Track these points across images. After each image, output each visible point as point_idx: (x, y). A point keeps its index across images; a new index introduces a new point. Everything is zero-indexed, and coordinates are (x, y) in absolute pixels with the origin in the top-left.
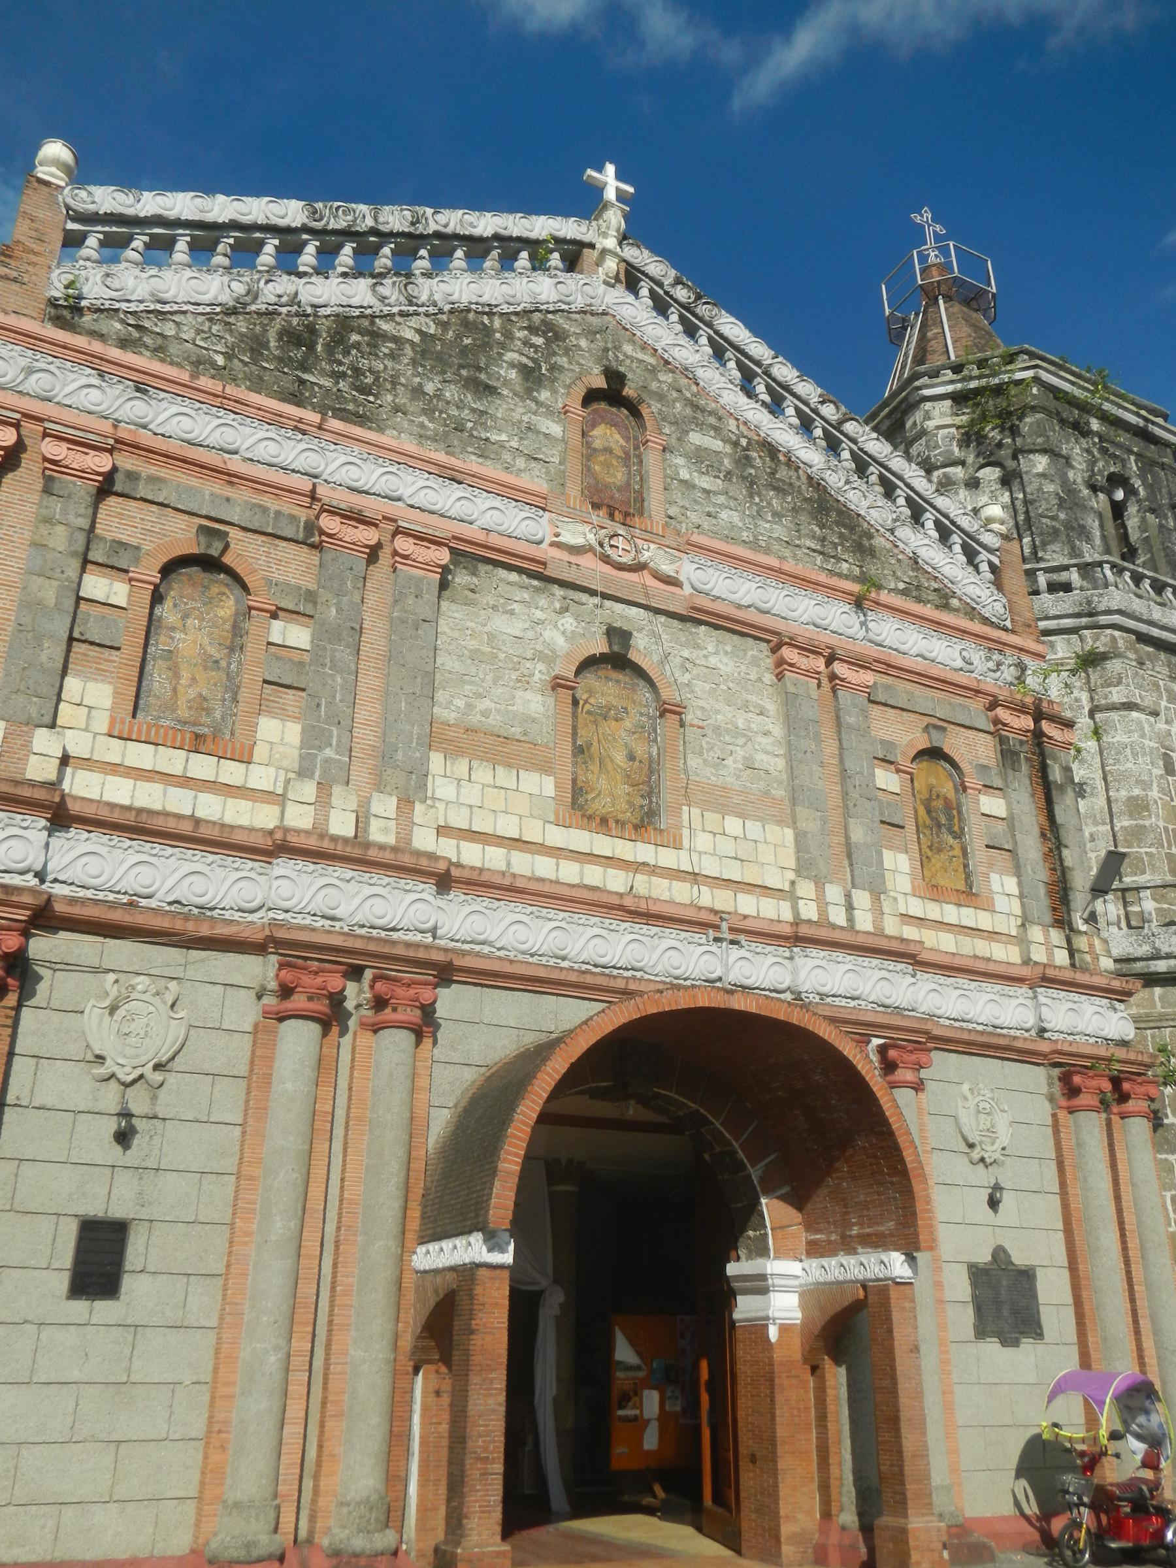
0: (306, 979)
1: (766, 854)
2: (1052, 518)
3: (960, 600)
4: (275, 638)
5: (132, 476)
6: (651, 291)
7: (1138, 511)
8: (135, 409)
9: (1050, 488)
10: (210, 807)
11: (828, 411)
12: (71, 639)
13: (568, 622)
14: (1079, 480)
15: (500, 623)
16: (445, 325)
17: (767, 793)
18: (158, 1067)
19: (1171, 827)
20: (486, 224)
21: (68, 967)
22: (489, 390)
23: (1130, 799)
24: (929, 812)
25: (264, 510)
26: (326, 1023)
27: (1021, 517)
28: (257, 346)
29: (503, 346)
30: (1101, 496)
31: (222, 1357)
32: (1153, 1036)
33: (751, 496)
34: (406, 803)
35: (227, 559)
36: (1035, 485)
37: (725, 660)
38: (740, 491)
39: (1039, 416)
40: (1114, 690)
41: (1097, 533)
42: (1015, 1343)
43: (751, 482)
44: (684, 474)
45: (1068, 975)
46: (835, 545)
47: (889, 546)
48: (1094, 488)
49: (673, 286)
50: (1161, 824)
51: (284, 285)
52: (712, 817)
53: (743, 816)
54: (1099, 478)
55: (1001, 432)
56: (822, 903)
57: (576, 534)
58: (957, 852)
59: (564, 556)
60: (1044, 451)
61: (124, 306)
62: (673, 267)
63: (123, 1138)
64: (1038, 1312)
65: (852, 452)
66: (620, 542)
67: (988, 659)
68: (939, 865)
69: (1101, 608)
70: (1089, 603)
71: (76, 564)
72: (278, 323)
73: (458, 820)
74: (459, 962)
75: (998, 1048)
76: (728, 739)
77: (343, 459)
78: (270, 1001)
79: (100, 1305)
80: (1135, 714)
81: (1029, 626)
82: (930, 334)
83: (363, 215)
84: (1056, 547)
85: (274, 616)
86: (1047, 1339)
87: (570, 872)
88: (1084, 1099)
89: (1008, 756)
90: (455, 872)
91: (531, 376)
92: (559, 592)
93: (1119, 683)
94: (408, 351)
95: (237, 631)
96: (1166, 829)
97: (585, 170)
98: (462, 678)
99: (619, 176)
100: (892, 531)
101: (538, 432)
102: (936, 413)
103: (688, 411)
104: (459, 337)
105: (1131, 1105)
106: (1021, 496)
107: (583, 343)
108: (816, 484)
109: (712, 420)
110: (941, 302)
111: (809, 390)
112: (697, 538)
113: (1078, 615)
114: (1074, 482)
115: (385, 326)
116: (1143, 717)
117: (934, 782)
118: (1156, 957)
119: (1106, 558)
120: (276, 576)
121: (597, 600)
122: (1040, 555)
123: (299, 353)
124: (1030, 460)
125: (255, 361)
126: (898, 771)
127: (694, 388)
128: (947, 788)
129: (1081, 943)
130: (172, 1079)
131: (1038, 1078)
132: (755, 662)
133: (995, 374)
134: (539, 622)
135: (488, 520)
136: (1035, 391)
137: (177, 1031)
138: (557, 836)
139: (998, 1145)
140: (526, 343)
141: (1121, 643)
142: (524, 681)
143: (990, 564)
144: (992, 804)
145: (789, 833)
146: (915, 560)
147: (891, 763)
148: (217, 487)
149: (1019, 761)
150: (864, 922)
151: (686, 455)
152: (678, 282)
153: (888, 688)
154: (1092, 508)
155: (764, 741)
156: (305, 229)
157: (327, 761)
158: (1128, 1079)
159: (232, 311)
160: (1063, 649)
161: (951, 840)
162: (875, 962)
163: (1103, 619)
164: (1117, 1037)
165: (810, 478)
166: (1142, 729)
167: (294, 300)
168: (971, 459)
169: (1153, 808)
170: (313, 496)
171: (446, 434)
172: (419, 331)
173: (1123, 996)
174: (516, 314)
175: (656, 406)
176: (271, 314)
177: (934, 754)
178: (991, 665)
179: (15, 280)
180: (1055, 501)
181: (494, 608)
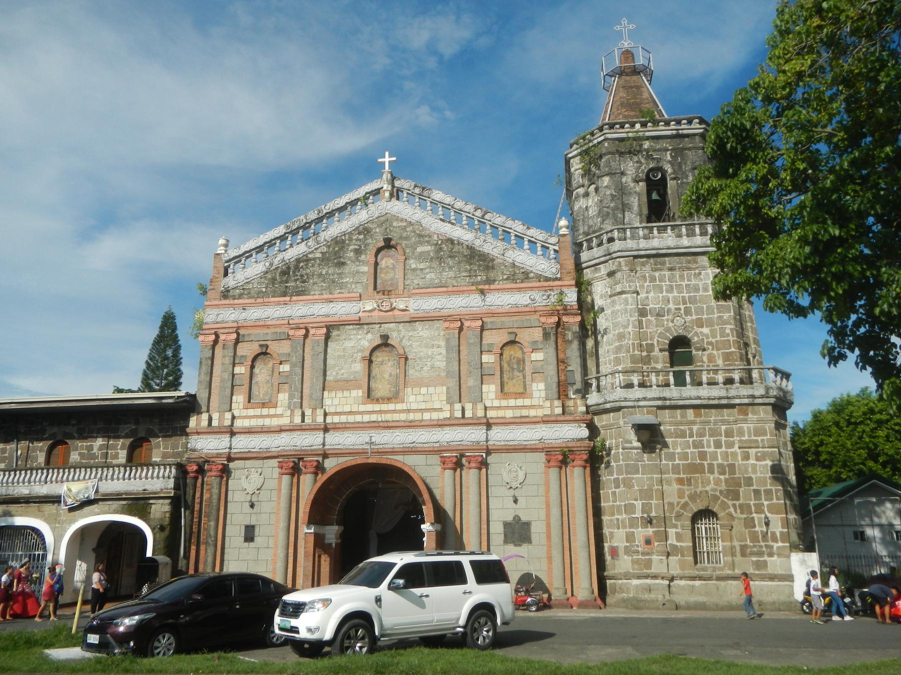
0: (284, 465)
1: (435, 397)
2: (608, 207)
4: (281, 370)
5: (244, 336)
6: (408, 193)
8: (244, 315)
10: (267, 422)
11: (479, 213)
12: (233, 386)
13: (370, 336)
14: (630, 180)
15: (349, 344)
16: (329, 247)
18: (258, 490)
20: (341, 202)
21: (238, 469)
22: (343, 264)
23: (619, 334)
24: (509, 365)
25: (277, 333)
26: (293, 475)
28: (273, 280)
29: (349, 245)
30: (641, 184)
31: (275, 555)
33: (440, 264)
34: (314, 410)
35: (268, 351)
37: (426, 332)
38: (435, 264)
39: (607, 157)
40: (617, 286)
42: (520, 545)
43: (440, 259)
44: (414, 266)
45: (563, 418)
46: (475, 271)
47: (501, 261)
49: (414, 189)
50: (630, 342)
51: (280, 256)
52: (416, 390)
53: (428, 386)
56: (452, 411)
57: (368, 307)
58: (521, 377)
59: (368, 314)
60: (607, 175)
61: (239, 285)
62: (413, 181)
63: (252, 506)
65: (491, 226)
66: (384, 304)
67: (543, 295)
69: (612, 251)
71: (231, 366)
72: (279, 270)
73: (332, 410)
74: (327, 452)
75: (520, 449)
77: (297, 308)
78: (280, 470)
79: (251, 544)
80: (624, 296)
83: (303, 220)
85: (281, 364)
87: (366, 418)
88: (552, 463)
89: (546, 335)
90: (329, 427)
91: (358, 252)
92: (366, 327)
94: (318, 262)
95: (273, 371)
96: (633, 344)
98: (335, 366)
99: (390, 157)
100: (503, 255)
101: (359, 272)
102: (574, 164)
103: (417, 239)
104: (334, 249)
107: (377, 230)
108: (471, 248)
109: (427, 239)
111: (470, 208)
112: (414, 291)
113: (605, 256)
115: (310, 256)
116: (629, 295)
117: (512, 352)
118: (606, 403)
119: (614, 227)
120: (282, 351)
121: (379, 325)
123: (285, 278)
125: (273, 286)
127: (421, 228)
128: (519, 354)
129: (570, 403)
130: (262, 492)
131: (542, 457)
132: (438, 328)
133: (590, 141)
134: (360, 339)
135: (341, 312)
136: (606, 145)
137: (262, 480)
138: (362, 408)
140: (357, 240)
141: (623, 264)
142: (354, 361)
143: (555, 251)
144: (538, 356)
145: (445, 388)
146: (513, 265)
148: (266, 331)
149: (550, 336)
151: (415, 258)
152: (416, 186)
153: (492, 322)
155: (439, 357)
156: (286, 233)
157: (295, 402)
159: (267, 272)
161: (518, 374)
162: (469, 428)
163: (614, 255)
164: (579, 437)
165: (467, 246)
167: (283, 260)
168: (586, 183)
169: (627, 336)
170: (289, 324)
171: (329, 286)
172: (322, 253)
175: (404, 243)
176: (277, 268)
177: (512, 342)
178: (545, 297)
179: (214, 289)
180: (610, 198)
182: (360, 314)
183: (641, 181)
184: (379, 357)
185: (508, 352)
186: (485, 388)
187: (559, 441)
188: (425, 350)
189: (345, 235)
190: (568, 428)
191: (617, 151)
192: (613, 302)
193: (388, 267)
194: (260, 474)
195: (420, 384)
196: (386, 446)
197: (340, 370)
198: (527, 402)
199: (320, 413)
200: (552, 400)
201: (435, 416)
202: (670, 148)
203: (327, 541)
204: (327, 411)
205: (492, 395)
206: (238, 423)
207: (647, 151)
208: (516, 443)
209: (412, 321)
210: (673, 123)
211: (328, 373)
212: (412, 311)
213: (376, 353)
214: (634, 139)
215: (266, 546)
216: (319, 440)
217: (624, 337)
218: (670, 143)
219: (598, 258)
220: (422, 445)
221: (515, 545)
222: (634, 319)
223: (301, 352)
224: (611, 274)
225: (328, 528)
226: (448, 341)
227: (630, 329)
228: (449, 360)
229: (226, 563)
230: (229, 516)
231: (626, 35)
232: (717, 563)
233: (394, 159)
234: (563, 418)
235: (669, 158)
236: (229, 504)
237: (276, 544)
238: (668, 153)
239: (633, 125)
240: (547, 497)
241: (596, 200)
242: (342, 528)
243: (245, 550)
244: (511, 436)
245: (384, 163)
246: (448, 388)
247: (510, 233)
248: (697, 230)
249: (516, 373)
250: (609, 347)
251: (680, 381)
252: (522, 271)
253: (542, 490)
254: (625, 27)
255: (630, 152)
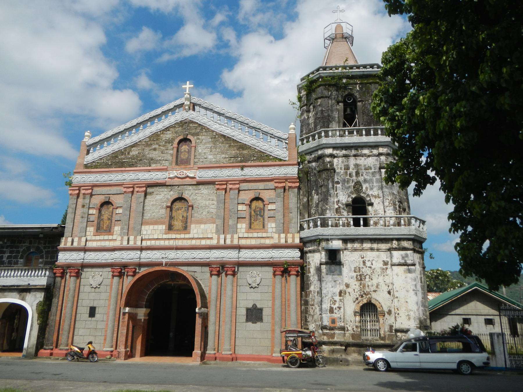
3: (273, 156)
13: (172, 193)
15: (158, 197)
17: (212, 217)
18: (99, 285)
24: (255, 212)
31: (107, 324)
35: (110, 201)
42: (256, 323)
56: (219, 239)
58: (262, 220)
64: (262, 317)
68: (256, 224)
73: (147, 237)
76: (204, 208)
85: (117, 209)
86: (264, 321)
87: (167, 243)
88: (277, 273)
92: (169, 187)
99: (190, 84)
126: (246, 205)
136: (320, 80)
137: (101, 280)
139: (257, 284)
145: (215, 225)
147: (244, 203)
150: (228, 242)
155: (212, 206)
157: (124, 232)
161: (260, 217)
172: (145, 142)
174: (166, 129)
181: (157, 194)
182: (166, 180)
184: (177, 205)
185: (255, 204)
186: (239, 226)
188: (204, 202)
189: (160, 131)
193: (185, 151)
194: (101, 276)
195: (200, 222)
196: (178, 260)
197: (153, 213)
198: (264, 235)
199: (139, 238)
201: (208, 242)
202: (359, 82)
203: (139, 318)
204: (143, 238)
205: (243, 230)
206: (90, 245)
208: (256, 259)
209: (199, 183)
211: (145, 214)
212: (198, 178)
213: (175, 204)
215: (102, 319)
216: (138, 256)
220: (199, 260)
221: (253, 323)
223: (130, 201)
225: (139, 309)
226: (218, 196)
228: (218, 208)
229: (76, 330)
230: (80, 301)
232: (375, 336)
235: (358, 88)
236: (80, 293)
237: (108, 319)
238: (358, 86)
240: (273, 293)
242: (148, 310)
243: (89, 322)
244: (254, 255)
245: (186, 88)
246: (217, 225)
247: (259, 132)
248: (372, 132)
249: (259, 217)
251: (357, 223)
252: (265, 155)
253: (270, 289)
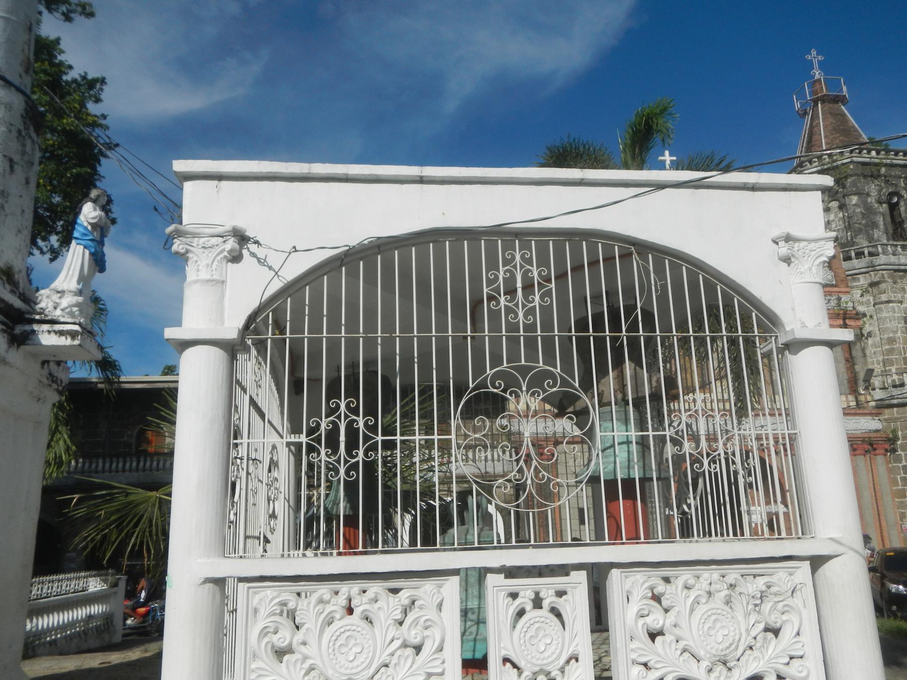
2: (859, 224)
7: (904, 204)
9: (858, 210)
14: (873, 201)
19: (906, 346)
27: (847, 224)
30: (884, 205)
32: (894, 425)
36: (852, 210)
39: (853, 178)
40: (883, 296)
41: (882, 223)
48: (880, 203)
50: (901, 346)
54: (883, 197)
55: (838, 186)
60: (855, 194)
69: (877, 264)
70: (872, 262)
80: (891, 305)
81: (843, 281)
82: (814, 124)
84: (861, 236)
88: (858, 452)
93: (885, 292)
96: (904, 348)
97: (658, 158)
99: (670, 155)
105: (877, 452)
106: (847, 214)
110: (819, 105)
114: (871, 203)
116: (895, 304)
122: (854, 240)
124: (850, 199)
129: (862, 398)
136: (851, 167)
141: (886, 276)
154: (879, 212)
158: (875, 444)
160: (863, 281)
163: (878, 268)
164: (874, 429)
166: (894, 309)
169: (898, 340)
173: (877, 414)
180: (860, 216)
183: (884, 203)
187: (858, 432)
190: (864, 421)
191: (862, 174)
192: (880, 309)
200: (846, 395)
202: (903, 176)
207: (885, 177)
210: (901, 154)
214: (876, 165)
217: (895, 341)
218: (900, 171)
219: (859, 269)
222: (901, 325)
224: (873, 285)
227: (899, 334)
231: (816, 65)
233: (674, 158)
234: (858, 411)
235: (903, 185)
238: (902, 180)
239: (869, 152)
241: (841, 215)
250: (875, 350)
254: (815, 58)
255: (872, 176)
